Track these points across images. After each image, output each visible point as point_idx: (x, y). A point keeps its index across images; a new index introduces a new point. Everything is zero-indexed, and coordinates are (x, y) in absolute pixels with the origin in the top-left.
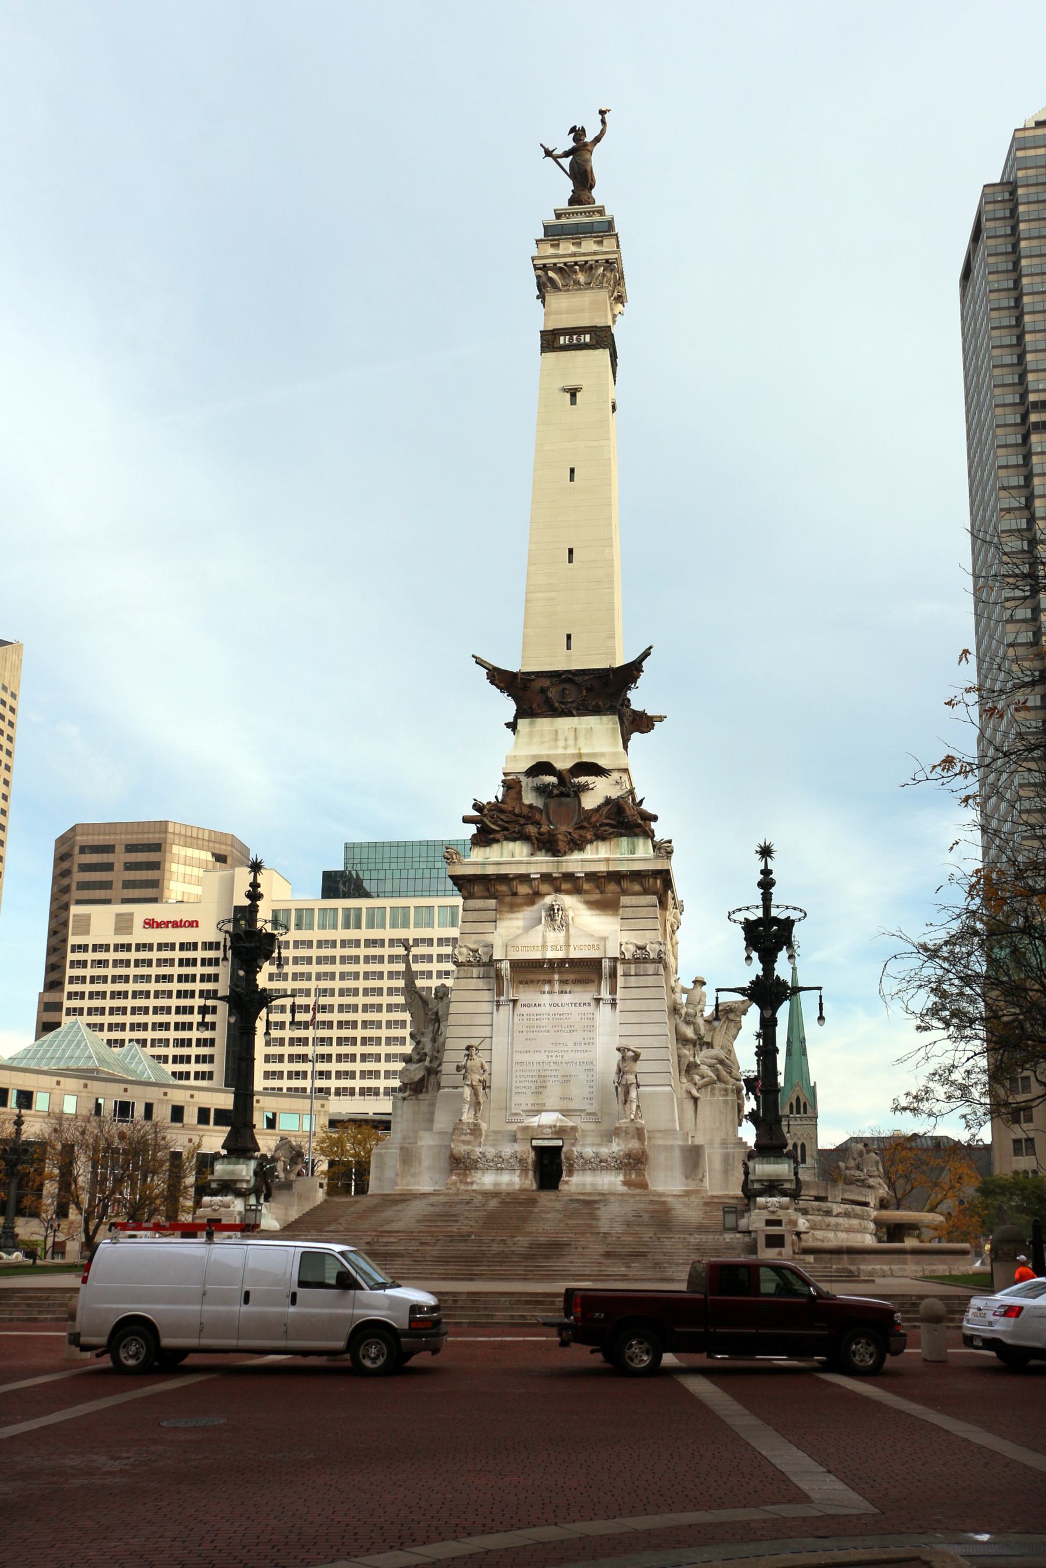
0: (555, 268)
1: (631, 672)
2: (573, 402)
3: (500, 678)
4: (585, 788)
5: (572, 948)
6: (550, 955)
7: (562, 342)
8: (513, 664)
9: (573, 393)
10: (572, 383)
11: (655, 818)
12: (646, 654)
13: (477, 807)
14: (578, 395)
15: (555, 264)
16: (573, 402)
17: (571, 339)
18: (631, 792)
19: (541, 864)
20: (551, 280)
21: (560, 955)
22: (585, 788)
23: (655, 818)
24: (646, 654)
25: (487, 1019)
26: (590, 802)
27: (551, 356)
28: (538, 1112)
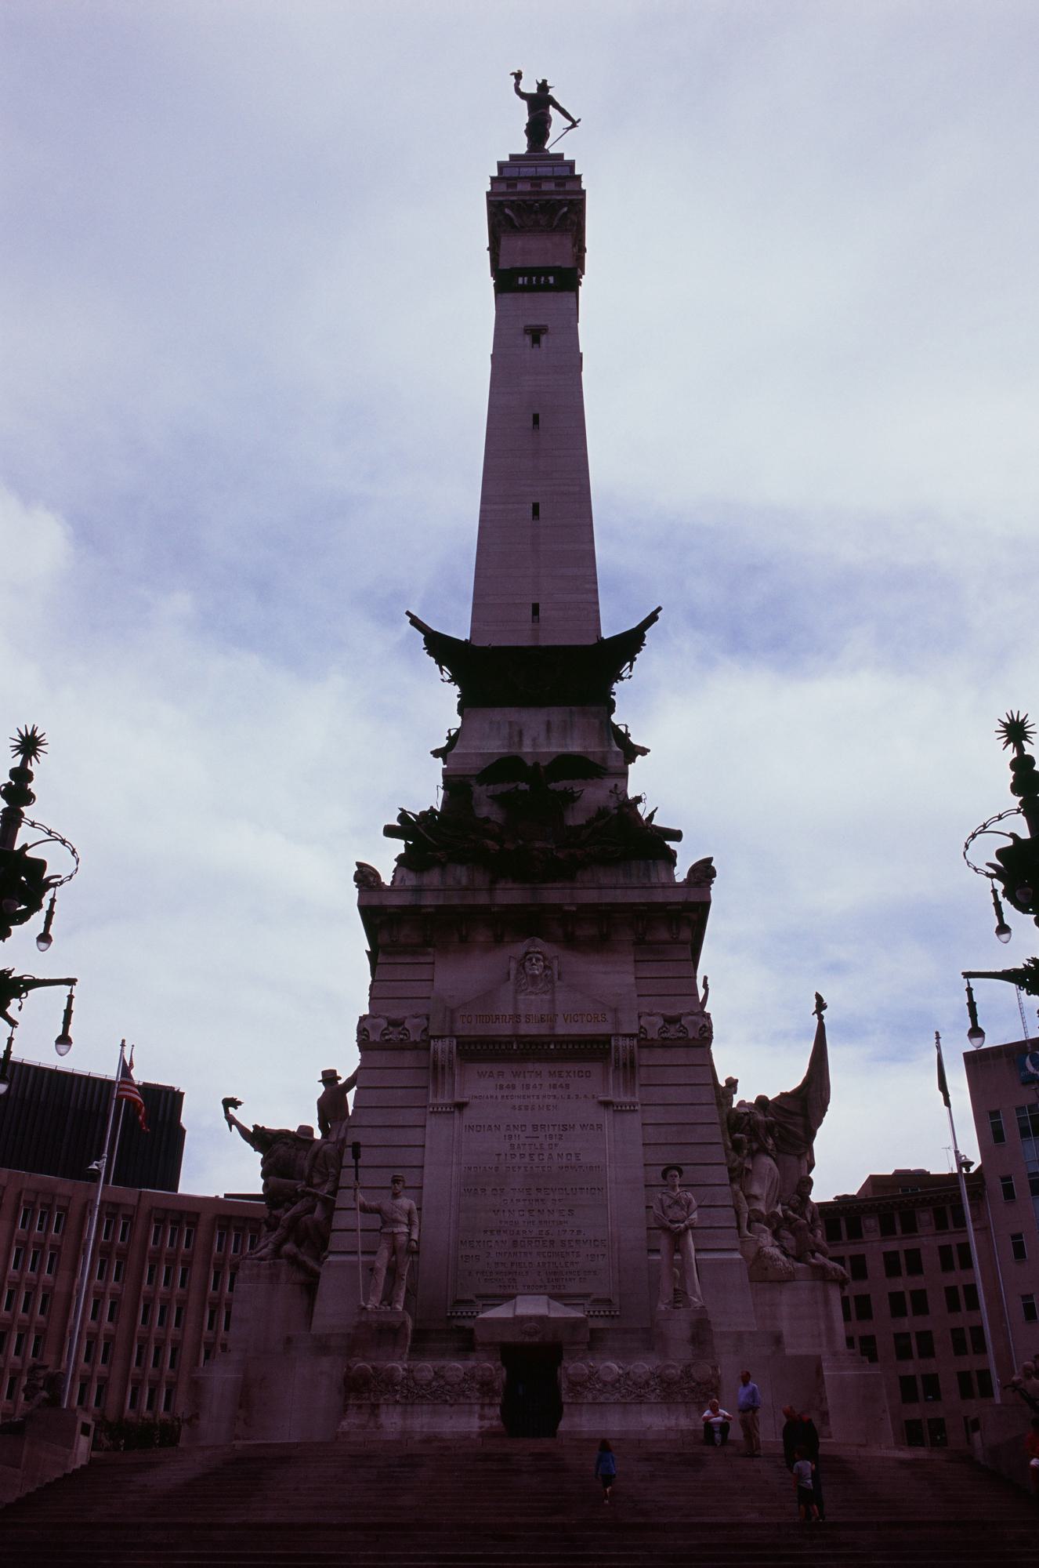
0: (512, 205)
3: (439, 646)
4: (570, 798)
5: (560, 1020)
6: (525, 1029)
7: (520, 280)
8: (460, 630)
9: (536, 334)
10: (533, 322)
11: (677, 836)
12: (653, 618)
13: (403, 816)
14: (543, 338)
15: (513, 202)
17: (530, 280)
20: (508, 218)
21: (542, 1029)
23: (677, 836)
24: (653, 618)
27: (508, 296)
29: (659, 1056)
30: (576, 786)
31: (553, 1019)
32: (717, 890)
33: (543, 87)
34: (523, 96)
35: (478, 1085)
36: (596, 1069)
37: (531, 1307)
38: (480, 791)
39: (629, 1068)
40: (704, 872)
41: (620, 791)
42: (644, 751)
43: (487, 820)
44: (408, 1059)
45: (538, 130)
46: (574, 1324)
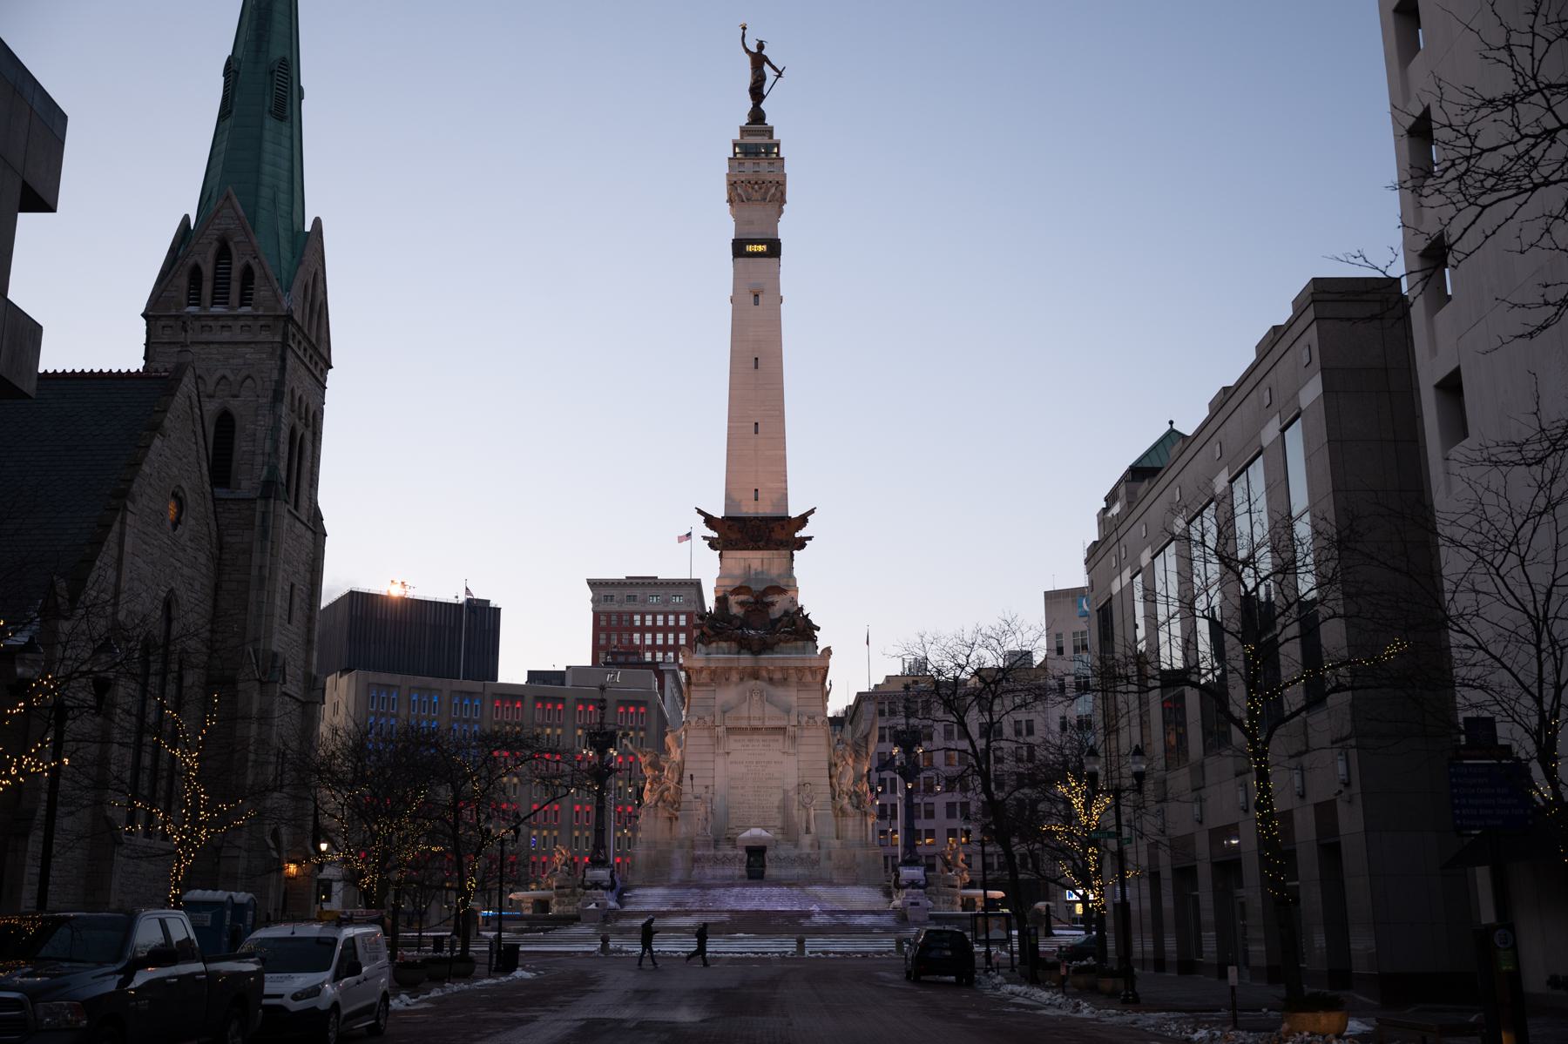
1: (803, 520)
2: (756, 303)
3: (710, 521)
4: (772, 604)
8: (718, 512)
12: (812, 511)
16: (756, 303)
18: (801, 609)
19: (746, 660)
22: (772, 604)
24: (812, 511)
25: (710, 765)
26: (776, 612)
27: (740, 260)
28: (749, 828)
29: (806, 733)
30: (776, 598)
31: (762, 719)
32: (832, 661)
33: (761, 46)
34: (747, 51)
35: (734, 744)
36: (781, 738)
37: (756, 832)
38: (733, 599)
39: (794, 738)
40: (828, 651)
41: (794, 601)
42: (810, 538)
43: (735, 616)
44: (706, 733)
45: (757, 93)
46: (770, 840)
